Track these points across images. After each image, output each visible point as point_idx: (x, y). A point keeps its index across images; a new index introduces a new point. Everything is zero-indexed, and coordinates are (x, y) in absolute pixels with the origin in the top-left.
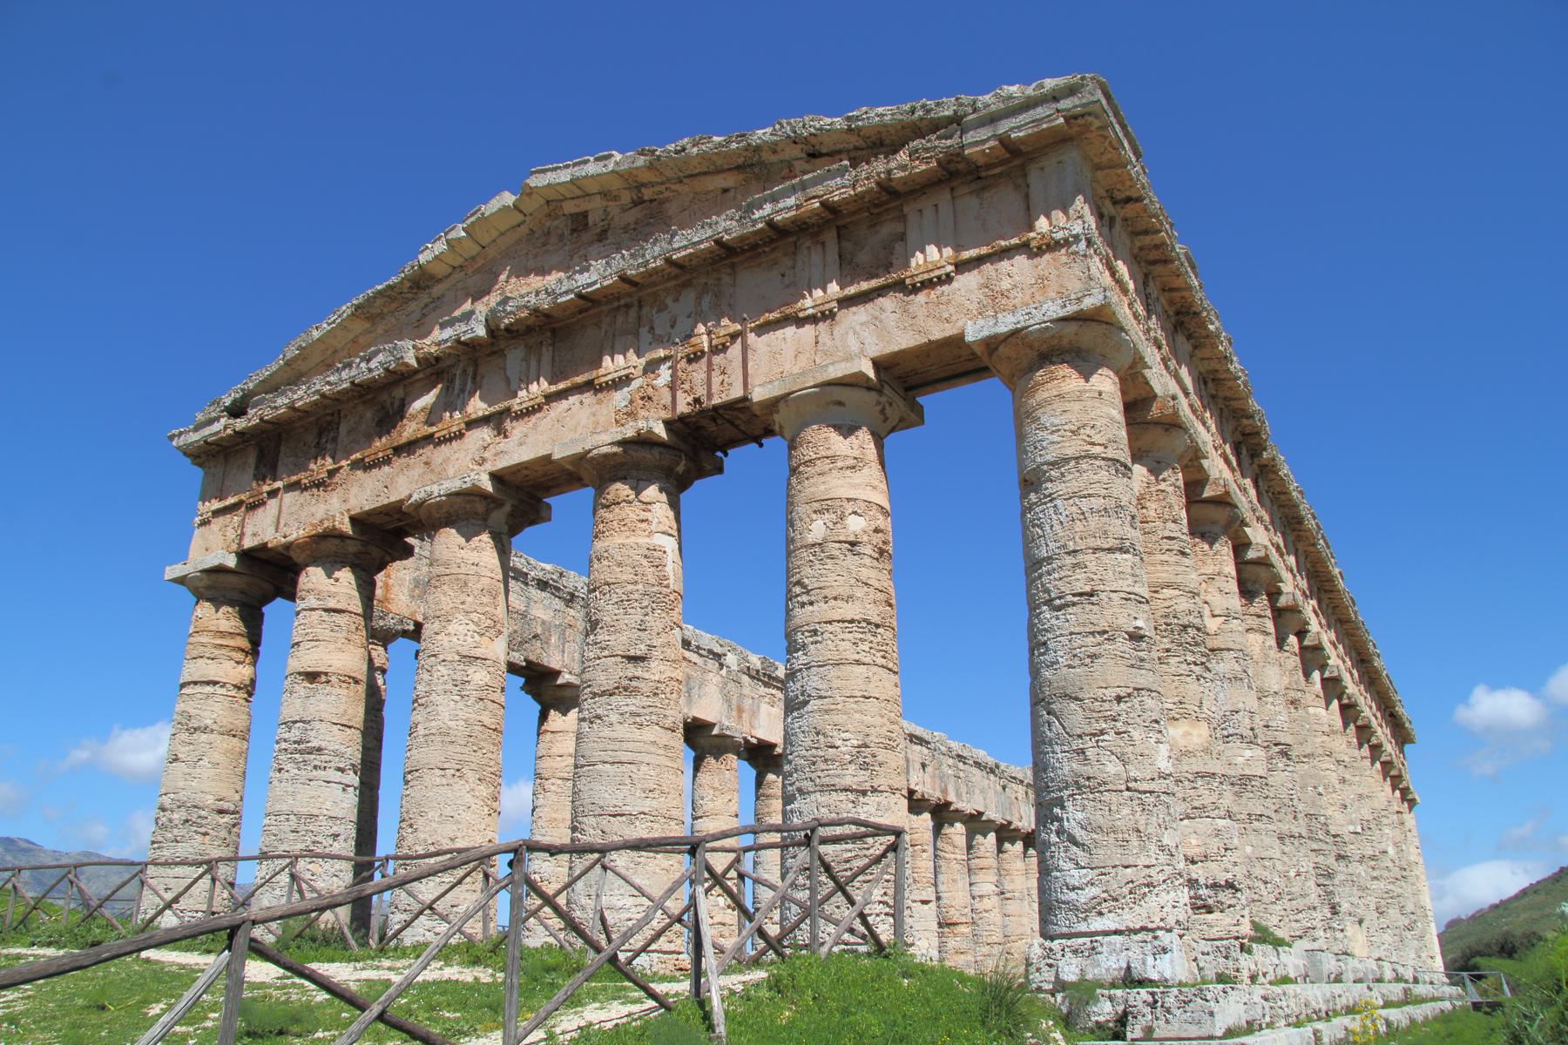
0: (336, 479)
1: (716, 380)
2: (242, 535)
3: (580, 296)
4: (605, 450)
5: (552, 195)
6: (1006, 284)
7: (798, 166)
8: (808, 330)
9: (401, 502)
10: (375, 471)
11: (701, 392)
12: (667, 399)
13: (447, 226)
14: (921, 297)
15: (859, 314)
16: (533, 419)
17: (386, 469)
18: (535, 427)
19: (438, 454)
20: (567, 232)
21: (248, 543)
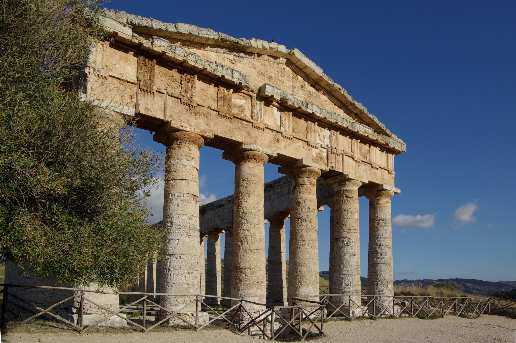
0: (197, 109)
1: (337, 164)
2: (136, 105)
3: (313, 113)
4: (317, 169)
5: (294, 60)
6: (384, 177)
7: (353, 114)
8: (354, 162)
9: (240, 144)
10: (223, 120)
11: (334, 165)
12: (326, 161)
13: (263, 39)
14: (373, 170)
15: (363, 167)
16: (289, 141)
17: (229, 123)
18: (289, 145)
19: (255, 132)
20: (291, 76)
21: (143, 111)
